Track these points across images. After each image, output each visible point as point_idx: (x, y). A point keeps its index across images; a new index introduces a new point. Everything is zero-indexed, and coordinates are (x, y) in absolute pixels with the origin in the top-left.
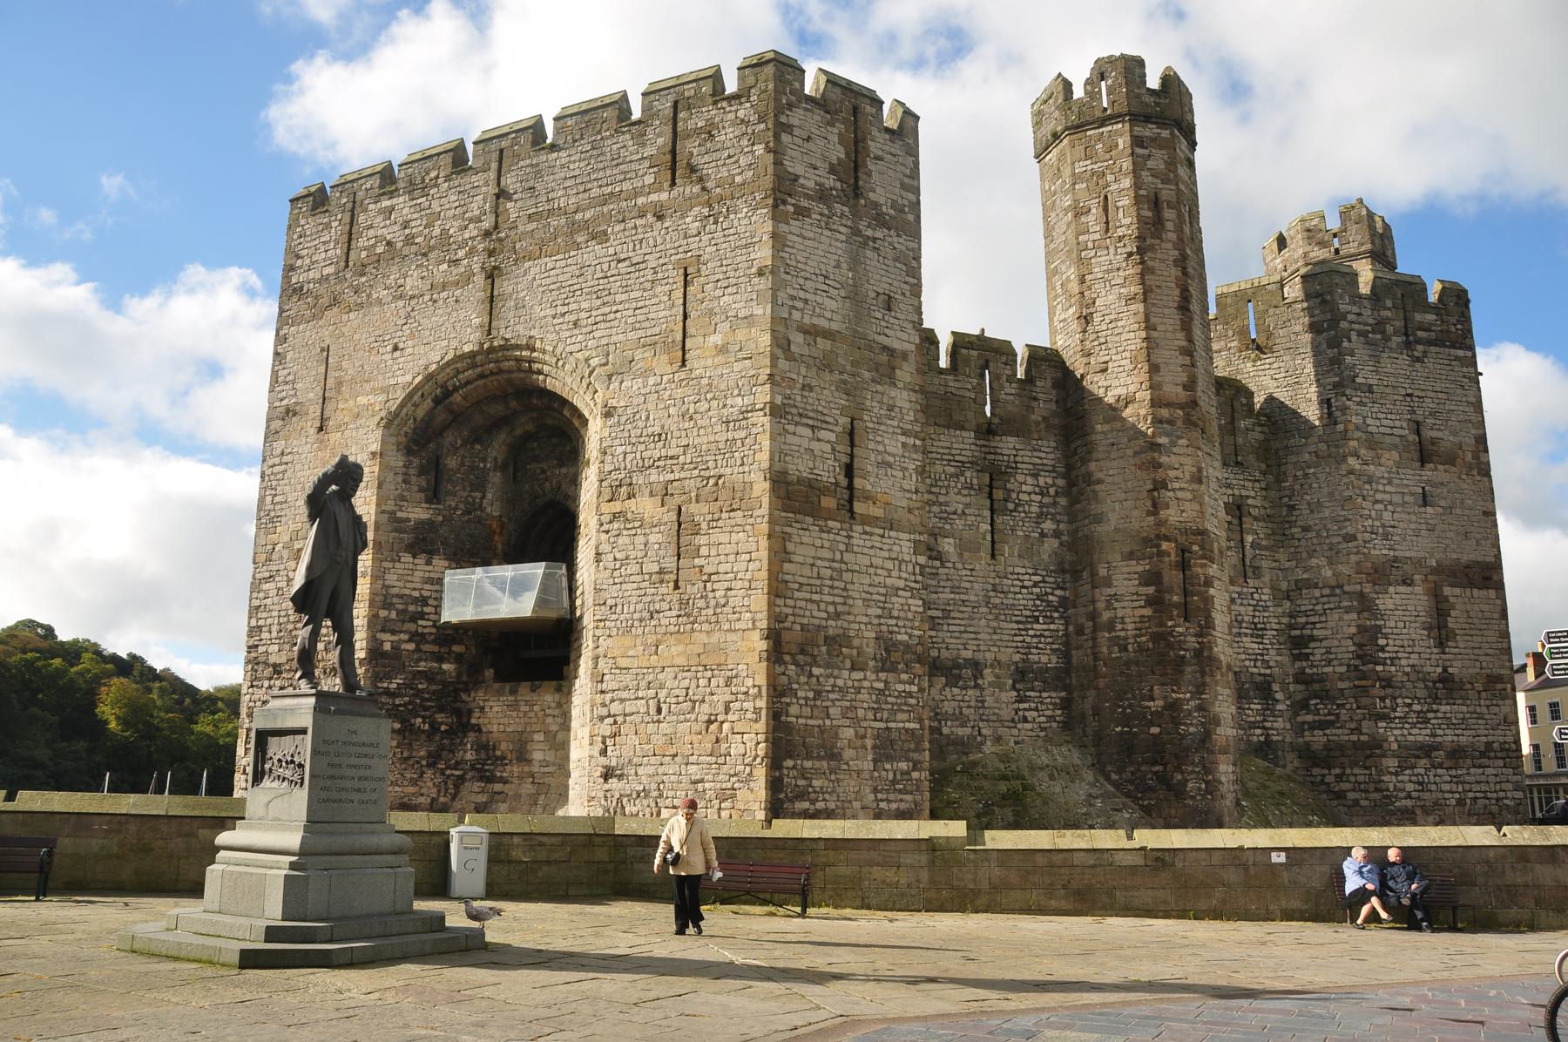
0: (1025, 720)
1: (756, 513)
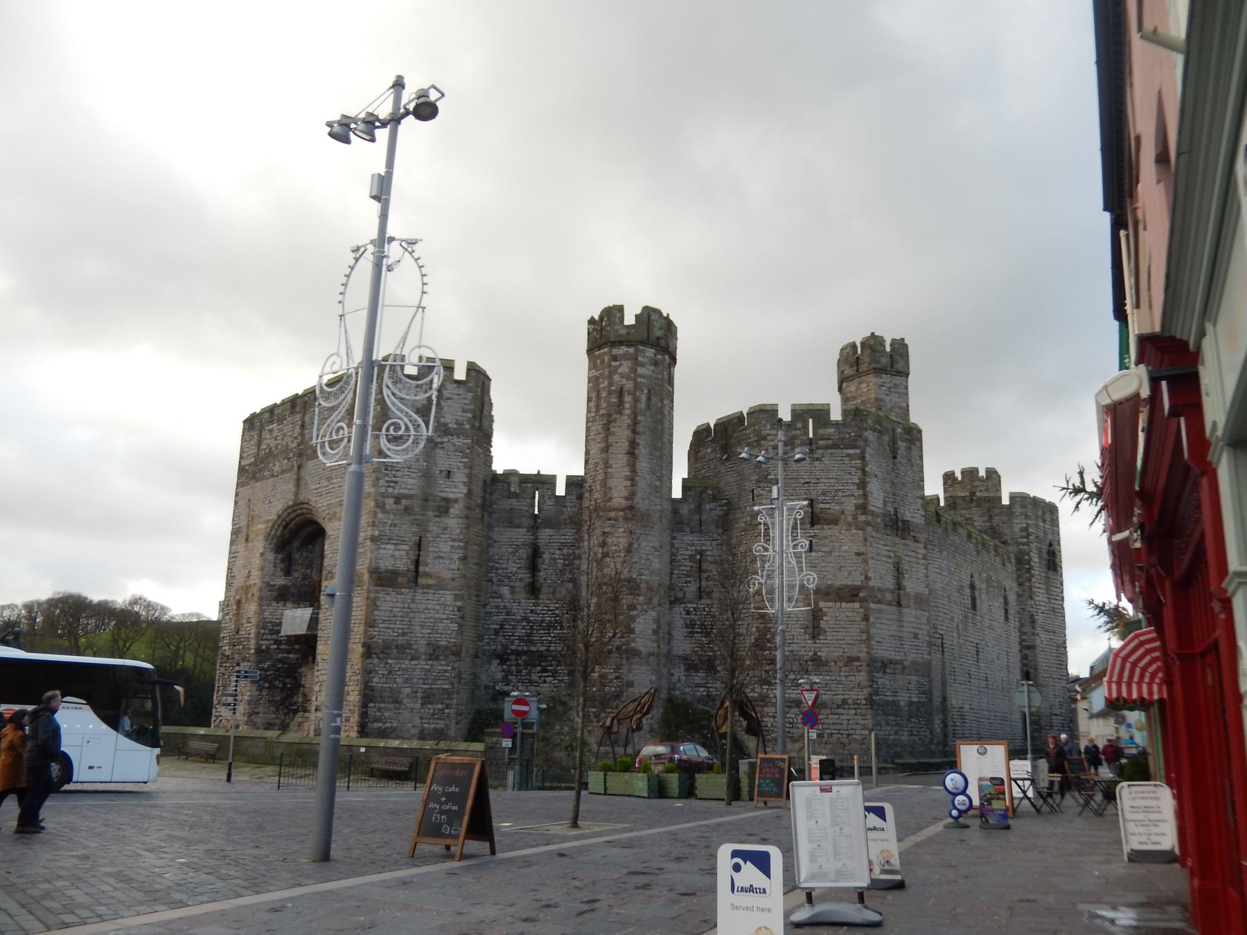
0: (545, 682)
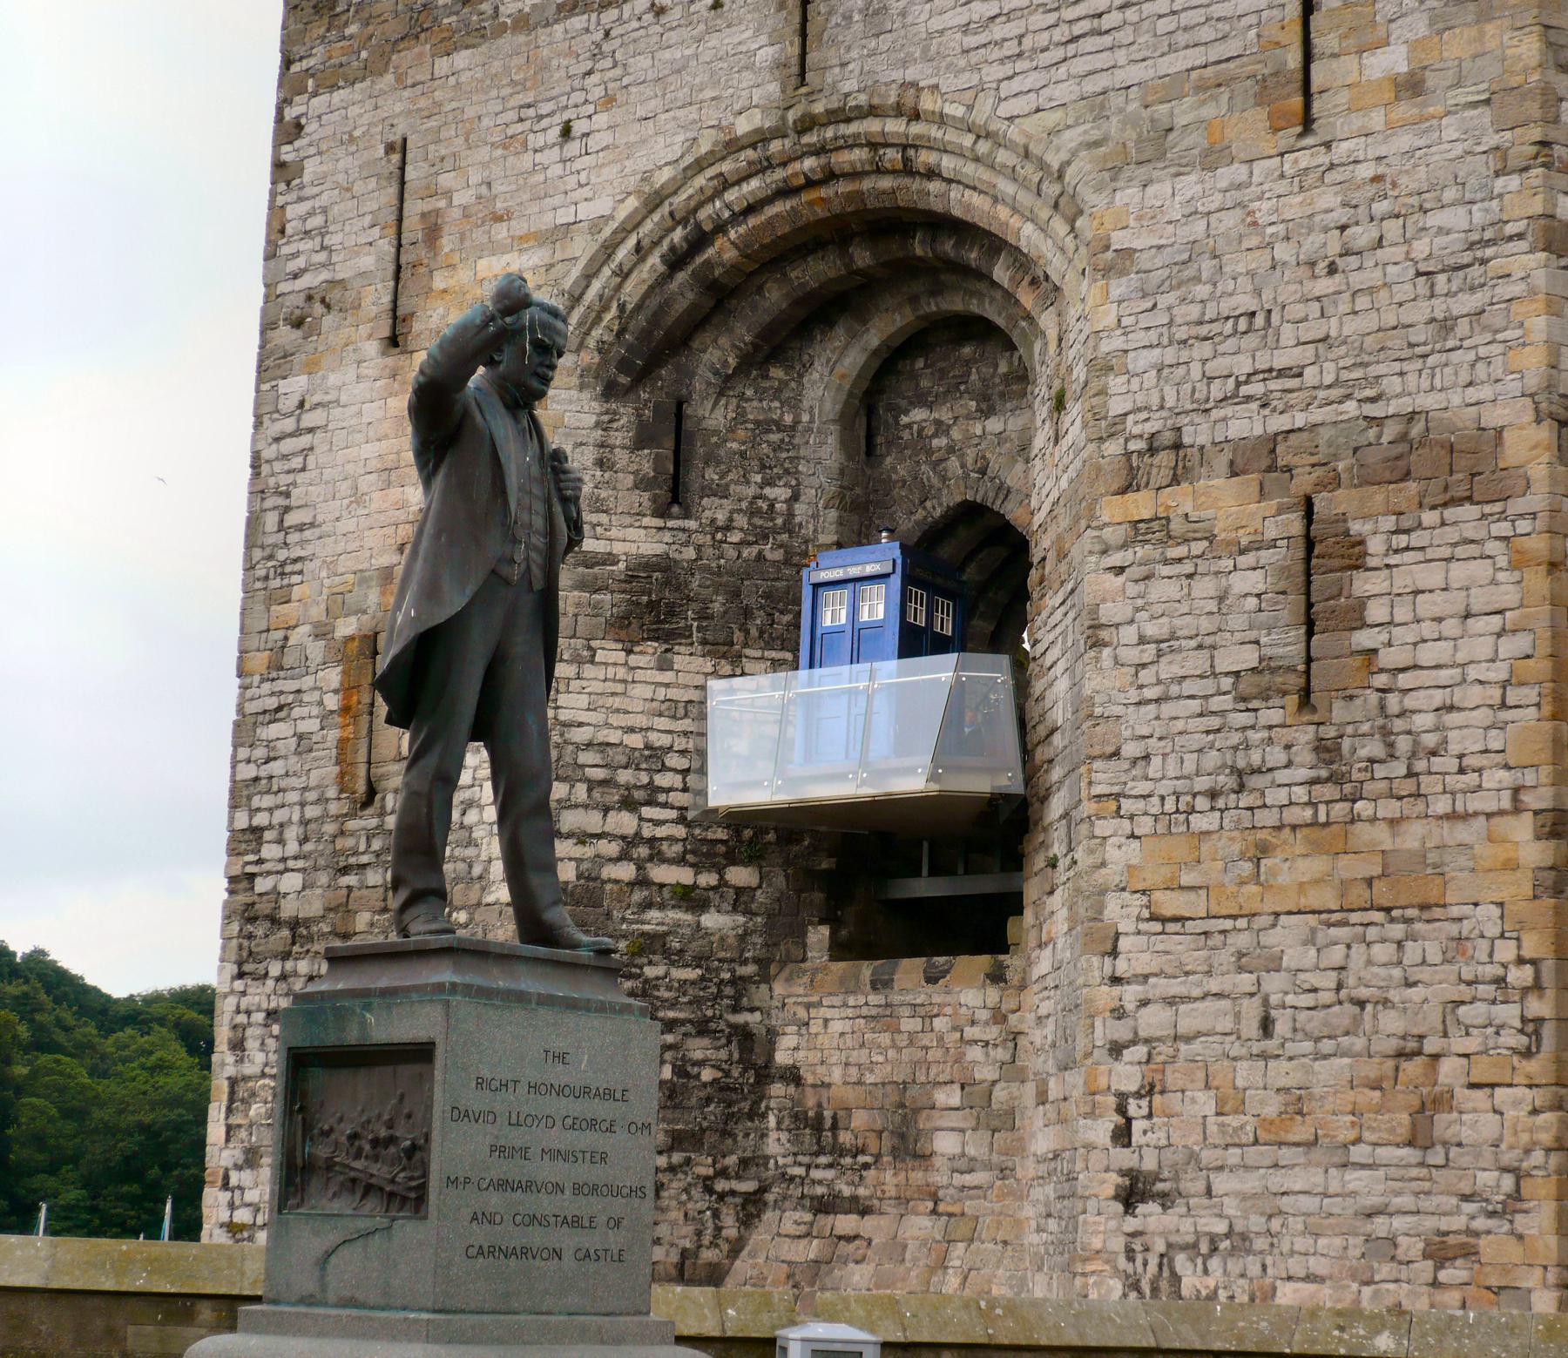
1: (1517, 506)
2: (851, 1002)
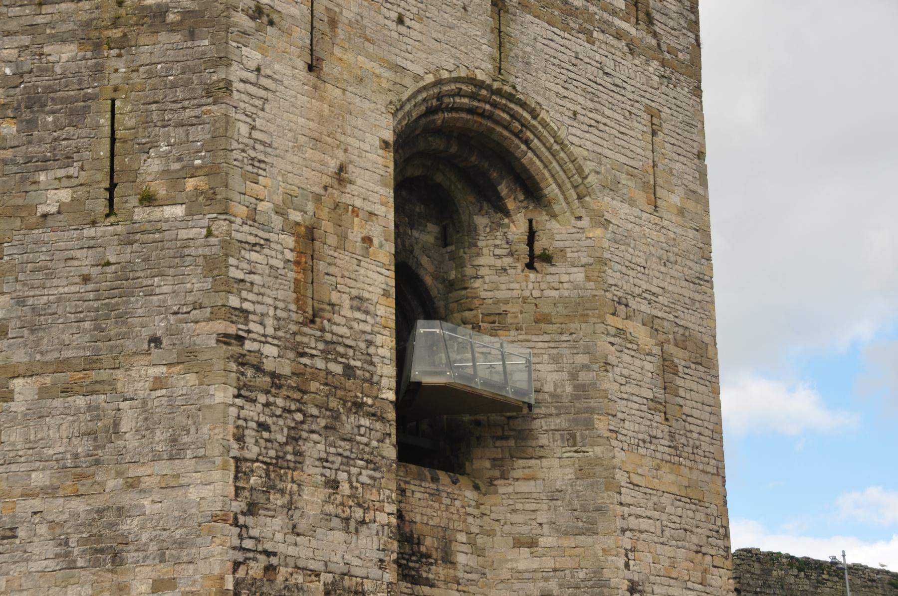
2: (423, 484)
